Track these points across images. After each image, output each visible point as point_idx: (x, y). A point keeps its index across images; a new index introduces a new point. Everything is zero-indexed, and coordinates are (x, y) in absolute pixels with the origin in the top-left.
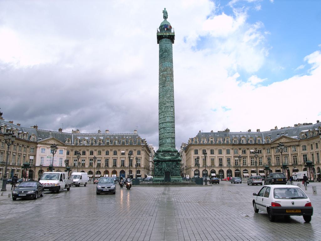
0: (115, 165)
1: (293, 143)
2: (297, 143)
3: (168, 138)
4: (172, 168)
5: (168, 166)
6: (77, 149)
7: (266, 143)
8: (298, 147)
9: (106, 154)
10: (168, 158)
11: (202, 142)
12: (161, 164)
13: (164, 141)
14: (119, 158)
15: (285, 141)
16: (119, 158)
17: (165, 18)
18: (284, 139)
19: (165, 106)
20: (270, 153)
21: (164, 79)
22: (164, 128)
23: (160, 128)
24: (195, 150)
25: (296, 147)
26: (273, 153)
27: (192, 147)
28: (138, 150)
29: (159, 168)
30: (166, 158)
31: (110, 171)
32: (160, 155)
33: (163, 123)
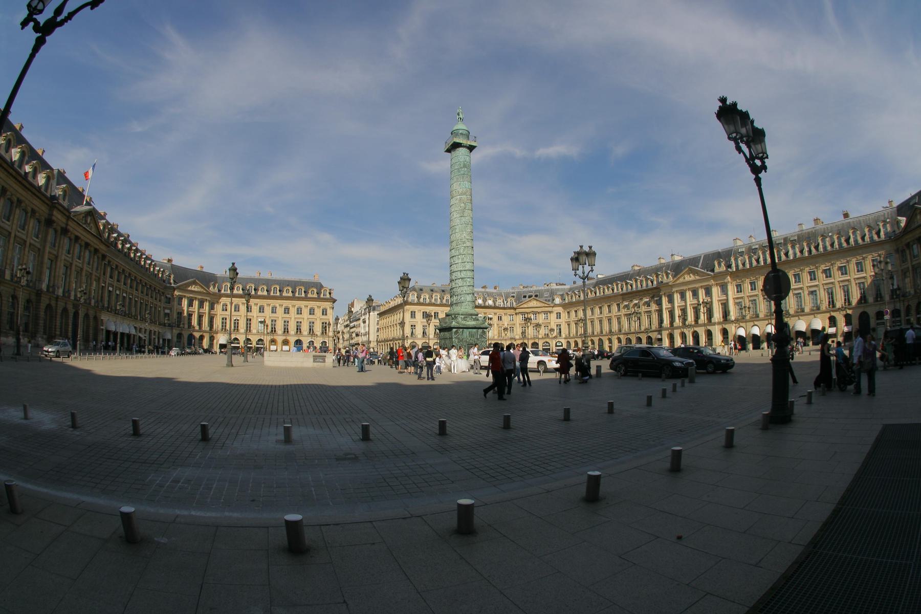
0: (286, 331)
1: (546, 308)
2: (550, 309)
3: (468, 294)
4: (477, 339)
5: (471, 335)
6: (429, 309)
7: (509, 306)
8: (551, 314)
9: (272, 312)
10: (472, 323)
11: (421, 300)
12: (463, 332)
13: (462, 299)
14: (293, 319)
15: (535, 305)
16: (293, 319)
17: (461, 119)
18: (535, 302)
19: (465, 245)
20: (536, 319)
21: (463, 205)
22: (462, 278)
23: (456, 278)
24: (412, 312)
25: (537, 314)
26: (518, 321)
27: (407, 307)
28: (324, 307)
29: (459, 339)
30: (467, 323)
31: (280, 339)
32: (460, 319)
33: (461, 271)
